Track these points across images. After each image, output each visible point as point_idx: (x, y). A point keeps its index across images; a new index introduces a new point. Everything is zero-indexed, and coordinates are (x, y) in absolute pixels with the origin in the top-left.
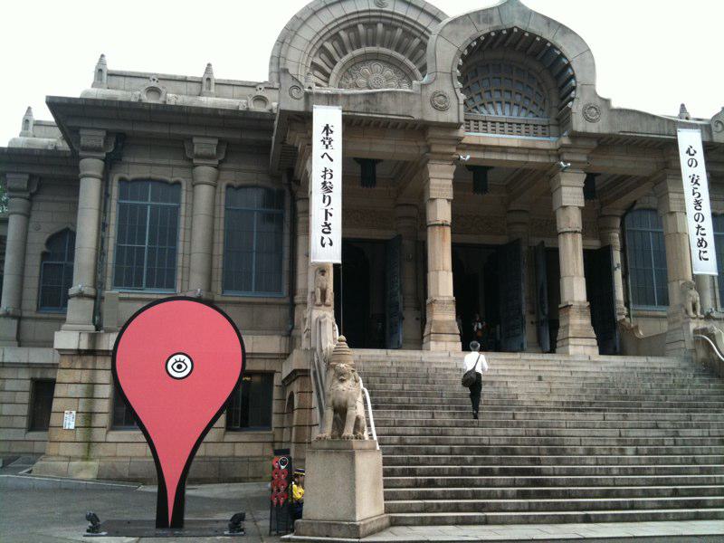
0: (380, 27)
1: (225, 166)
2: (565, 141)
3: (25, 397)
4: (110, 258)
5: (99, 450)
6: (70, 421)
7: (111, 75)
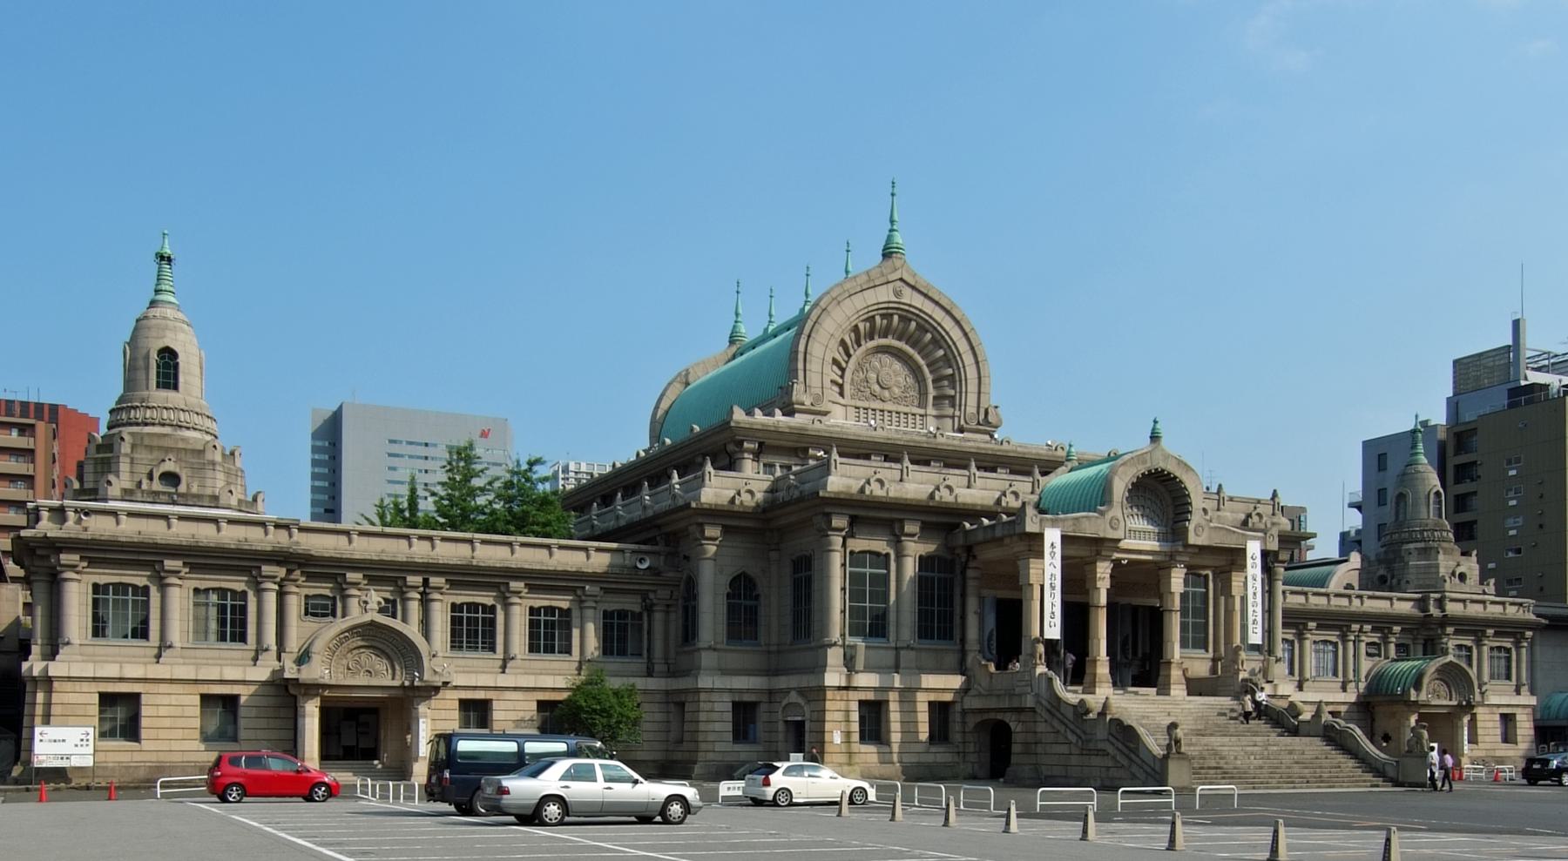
3: (729, 716)
5: (857, 759)
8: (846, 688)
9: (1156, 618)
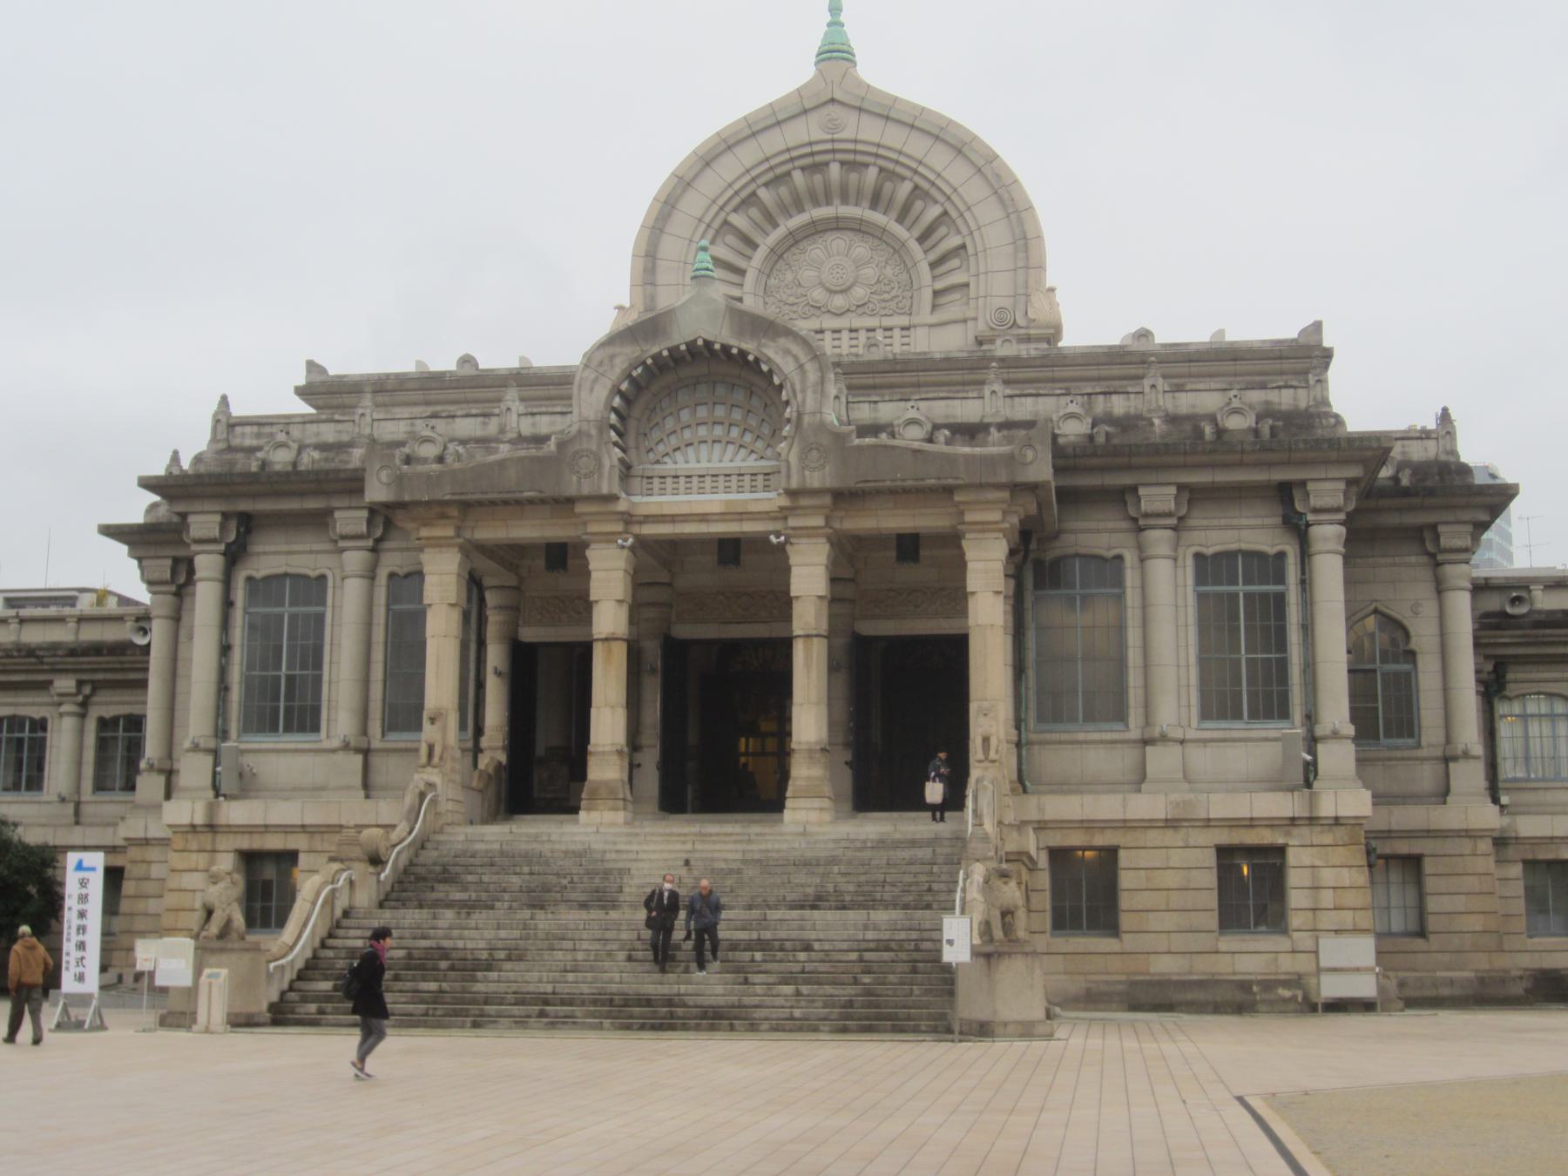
0: (835, 169)
1: (387, 545)
2: (784, 502)
4: (236, 695)
8: (212, 827)
9: (947, 659)
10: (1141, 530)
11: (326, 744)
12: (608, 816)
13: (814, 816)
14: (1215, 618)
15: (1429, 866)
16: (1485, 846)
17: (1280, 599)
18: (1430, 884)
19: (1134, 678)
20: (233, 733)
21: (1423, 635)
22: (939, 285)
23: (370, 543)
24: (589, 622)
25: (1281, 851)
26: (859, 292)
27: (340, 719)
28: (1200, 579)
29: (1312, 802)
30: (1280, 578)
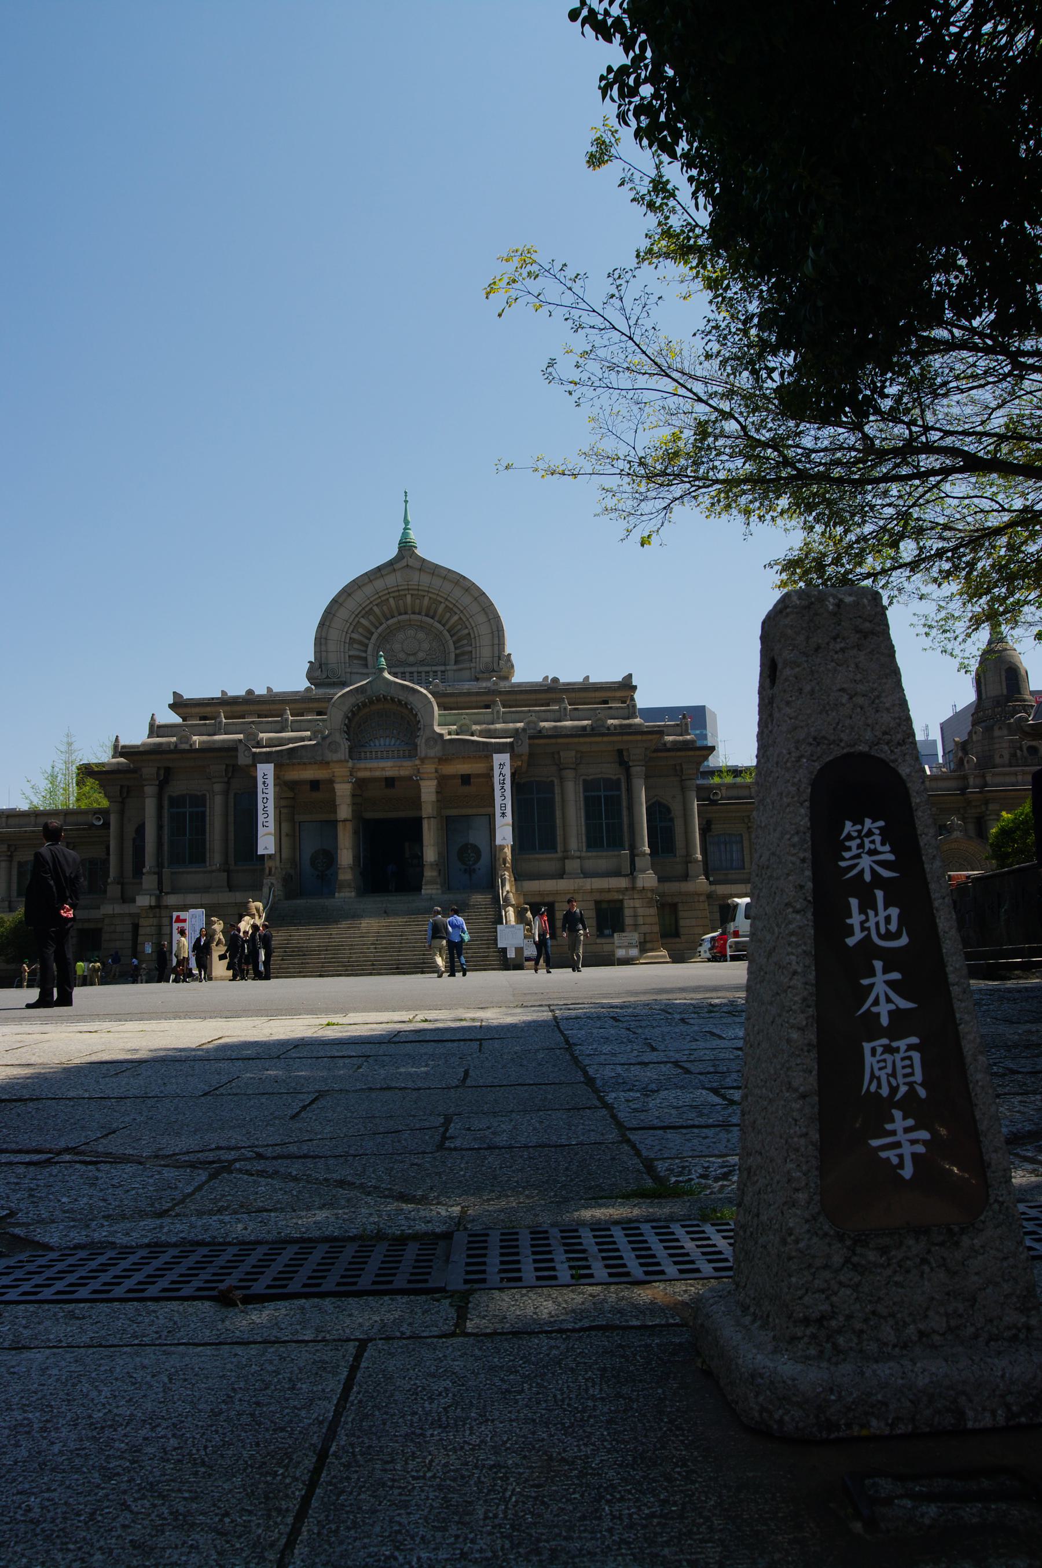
6: (148, 949)
7: (159, 727)
8: (158, 906)
10: (561, 769)
11: (209, 868)
12: (347, 894)
13: (434, 892)
14: (591, 805)
15: (680, 907)
16: (702, 898)
17: (619, 797)
18: (681, 914)
19: (559, 832)
20: (166, 865)
21: (676, 808)
22: (458, 651)
23: (226, 780)
24: (335, 812)
25: (621, 901)
26: (421, 655)
27: (216, 857)
28: (585, 791)
29: (634, 879)
30: (619, 789)
